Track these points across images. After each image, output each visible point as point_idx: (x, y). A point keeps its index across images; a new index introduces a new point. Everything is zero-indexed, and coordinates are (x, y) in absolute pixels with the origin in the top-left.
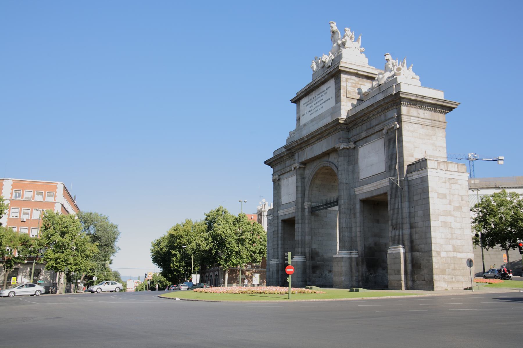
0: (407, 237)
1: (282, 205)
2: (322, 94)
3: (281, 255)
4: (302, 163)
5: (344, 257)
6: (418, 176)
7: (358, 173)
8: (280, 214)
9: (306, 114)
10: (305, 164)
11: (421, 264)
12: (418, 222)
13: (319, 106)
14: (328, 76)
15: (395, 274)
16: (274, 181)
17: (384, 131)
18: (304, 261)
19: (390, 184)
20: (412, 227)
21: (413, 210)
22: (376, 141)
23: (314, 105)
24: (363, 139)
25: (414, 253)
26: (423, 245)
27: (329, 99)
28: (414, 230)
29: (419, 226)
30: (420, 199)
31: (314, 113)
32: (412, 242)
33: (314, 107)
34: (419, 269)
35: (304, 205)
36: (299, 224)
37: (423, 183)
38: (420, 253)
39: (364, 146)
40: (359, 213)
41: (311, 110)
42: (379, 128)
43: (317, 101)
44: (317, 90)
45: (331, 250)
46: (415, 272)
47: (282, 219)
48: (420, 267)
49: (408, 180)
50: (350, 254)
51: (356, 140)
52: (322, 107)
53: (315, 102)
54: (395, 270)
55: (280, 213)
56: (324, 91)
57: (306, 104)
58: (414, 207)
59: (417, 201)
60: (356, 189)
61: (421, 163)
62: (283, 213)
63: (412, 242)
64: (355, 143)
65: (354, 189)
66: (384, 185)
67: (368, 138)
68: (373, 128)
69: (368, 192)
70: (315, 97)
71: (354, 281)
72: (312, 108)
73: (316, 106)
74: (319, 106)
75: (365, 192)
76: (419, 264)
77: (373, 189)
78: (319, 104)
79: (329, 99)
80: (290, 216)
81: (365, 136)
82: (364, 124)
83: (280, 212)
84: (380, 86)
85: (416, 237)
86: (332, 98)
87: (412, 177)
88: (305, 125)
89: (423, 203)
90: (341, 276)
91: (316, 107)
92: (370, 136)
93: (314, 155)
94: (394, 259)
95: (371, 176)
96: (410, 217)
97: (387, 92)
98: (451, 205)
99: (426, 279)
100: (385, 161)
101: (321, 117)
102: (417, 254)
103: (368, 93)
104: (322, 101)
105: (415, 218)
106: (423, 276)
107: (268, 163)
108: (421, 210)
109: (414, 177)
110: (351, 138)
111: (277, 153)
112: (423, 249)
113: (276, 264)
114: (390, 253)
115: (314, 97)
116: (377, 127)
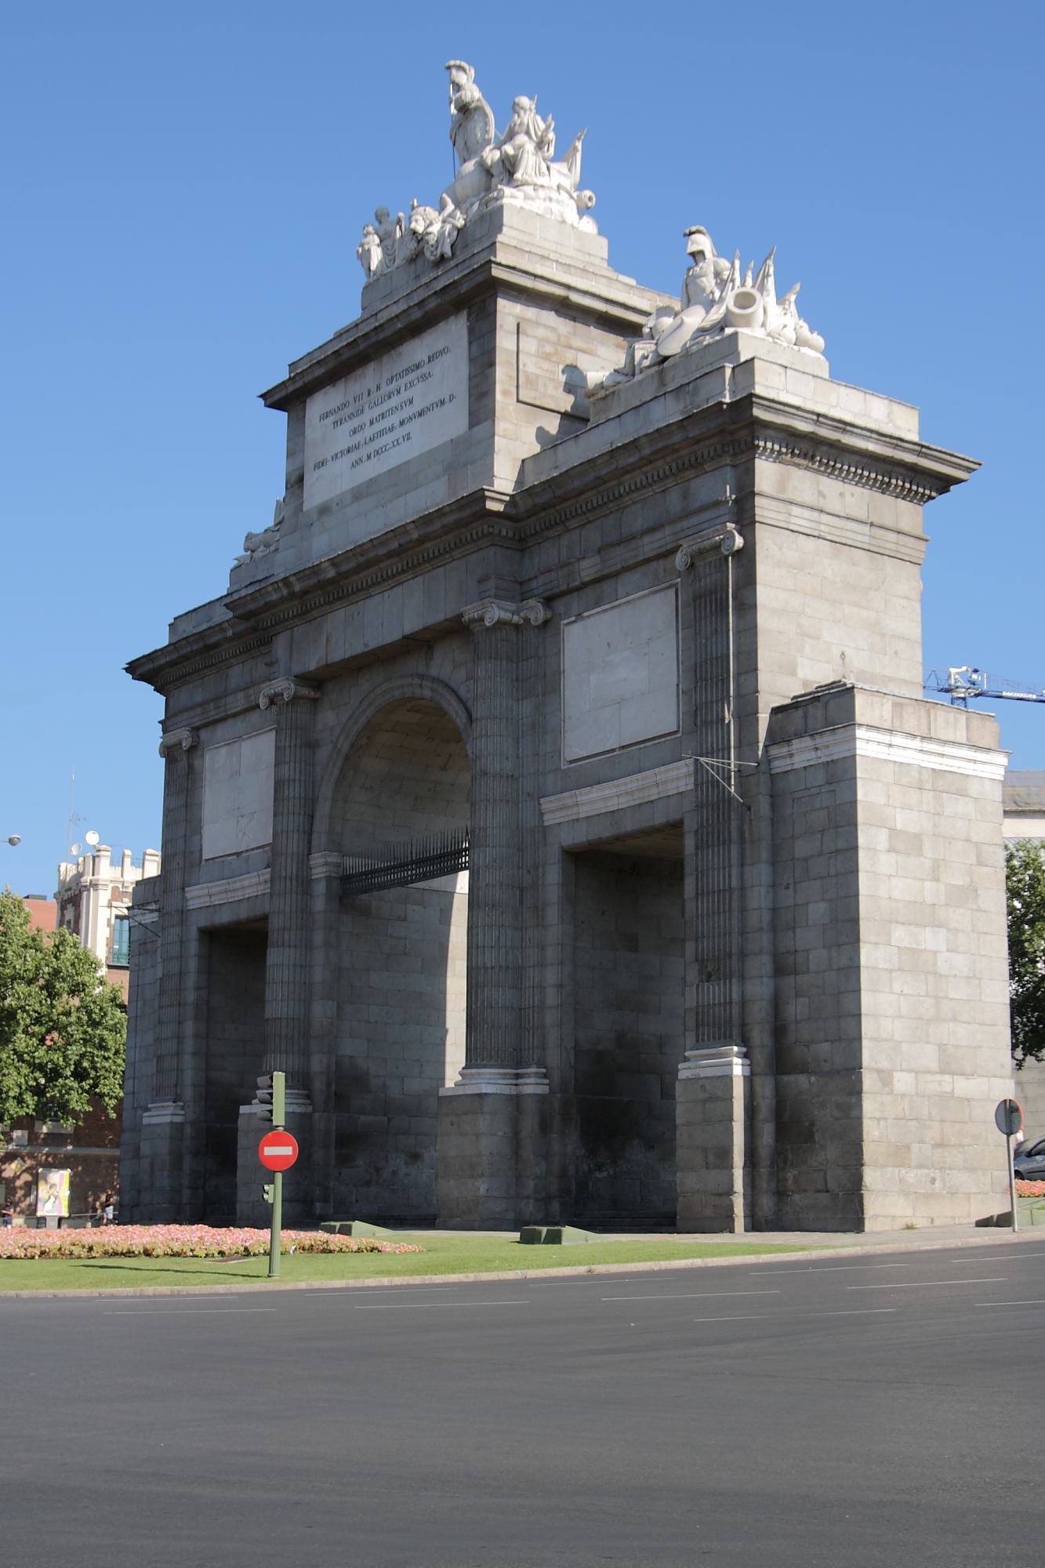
0: (759, 1011)
1: (203, 862)
3: (194, 1086)
4: (304, 679)
5: (486, 1094)
6: (813, 754)
7: (559, 732)
8: (197, 901)
9: (330, 463)
10: (318, 682)
11: (812, 1124)
12: (807, 951)
13: (392, 429)
14: (439, 300)
15: (707, 1168)
16: (169, 752)
17: (680, 560)
18: (300, 1113)
19: (696, 785)
20: (781, 969)
21: (787, 898)
22: (639, 598)
23: (372, 423)
24: (584, 585)
25: (786, 1078)
26: (826, 1046)
27: (442, 403)
28: (790, 980)
29: (812, 967)
31: (369, 457)
32: (779, 1030)
33: (369, 432)
34: (806, 1143)
35: (308, 864)
36: (292, 950)
37: (831, 788)
38: (813, 1079)
39: (588, 617)
40: (556, 906)
41: (357, 447)
42: (657, 545)
43: (384, 408)
44: (385, 358)
45: (422, 1066)
46: (790, 1157)
47: (202, 924)
48: (809, 1137)
49: (773, 772)
50: (514, 1082)
51: (557, 591)
52: (408, 437)
53: (377, 411)
54: (705, 1150)
55: (193, 898)
56: (418, 368)
57: (332, 418)
58: (791, 886)
59: (806, 859)
60: (547, 804)
61: (827, 704)
62: (208, 899)
63: (779, 1030)
64: (549, 601)
65: (539, 804)
66: (672, 789)
67: (607, 586)
69: (599, 815)
70: (378, 388)
71: (528, 1197)
72: (358, 438)
73: (378, 427)
74: (392, 429)
75: (587, 818)
76: (806, 1124)
77: (624, 802)
78: (394, 419)
79: (442, 403)
80: (244, 914)
81: (593, 577)
82: (589, 522)
83: (196, 893)
84: (666, 364)
85: (795, 1009)
86: (452, 397)
87: (788, 761)
88: (324, 510)
89: (833, 871)
90: (472, 1177)
91: (381, 433)
92: (616, 574)
93: (366, 645)
94: (705, 1101)
95: (613, 750)
96: (774, 928)
97: (696, 392)
98: (936, 879)
99: (831, 1184)
100: (678, 685)
101: (399, 479)
102: (801, 1082)
103: (611, 390)
104: (408, 411)
105: (798, 930)
106: (822, 1173)
107: (140, 669)
108: (823, 900)
109: (796, 759)
110: (530, 580)
111: (188, 629)
112: (825, 1061)
113: (172, 1122)
114: (688, 1079)
115: (373, 388)
116: (647, 539)
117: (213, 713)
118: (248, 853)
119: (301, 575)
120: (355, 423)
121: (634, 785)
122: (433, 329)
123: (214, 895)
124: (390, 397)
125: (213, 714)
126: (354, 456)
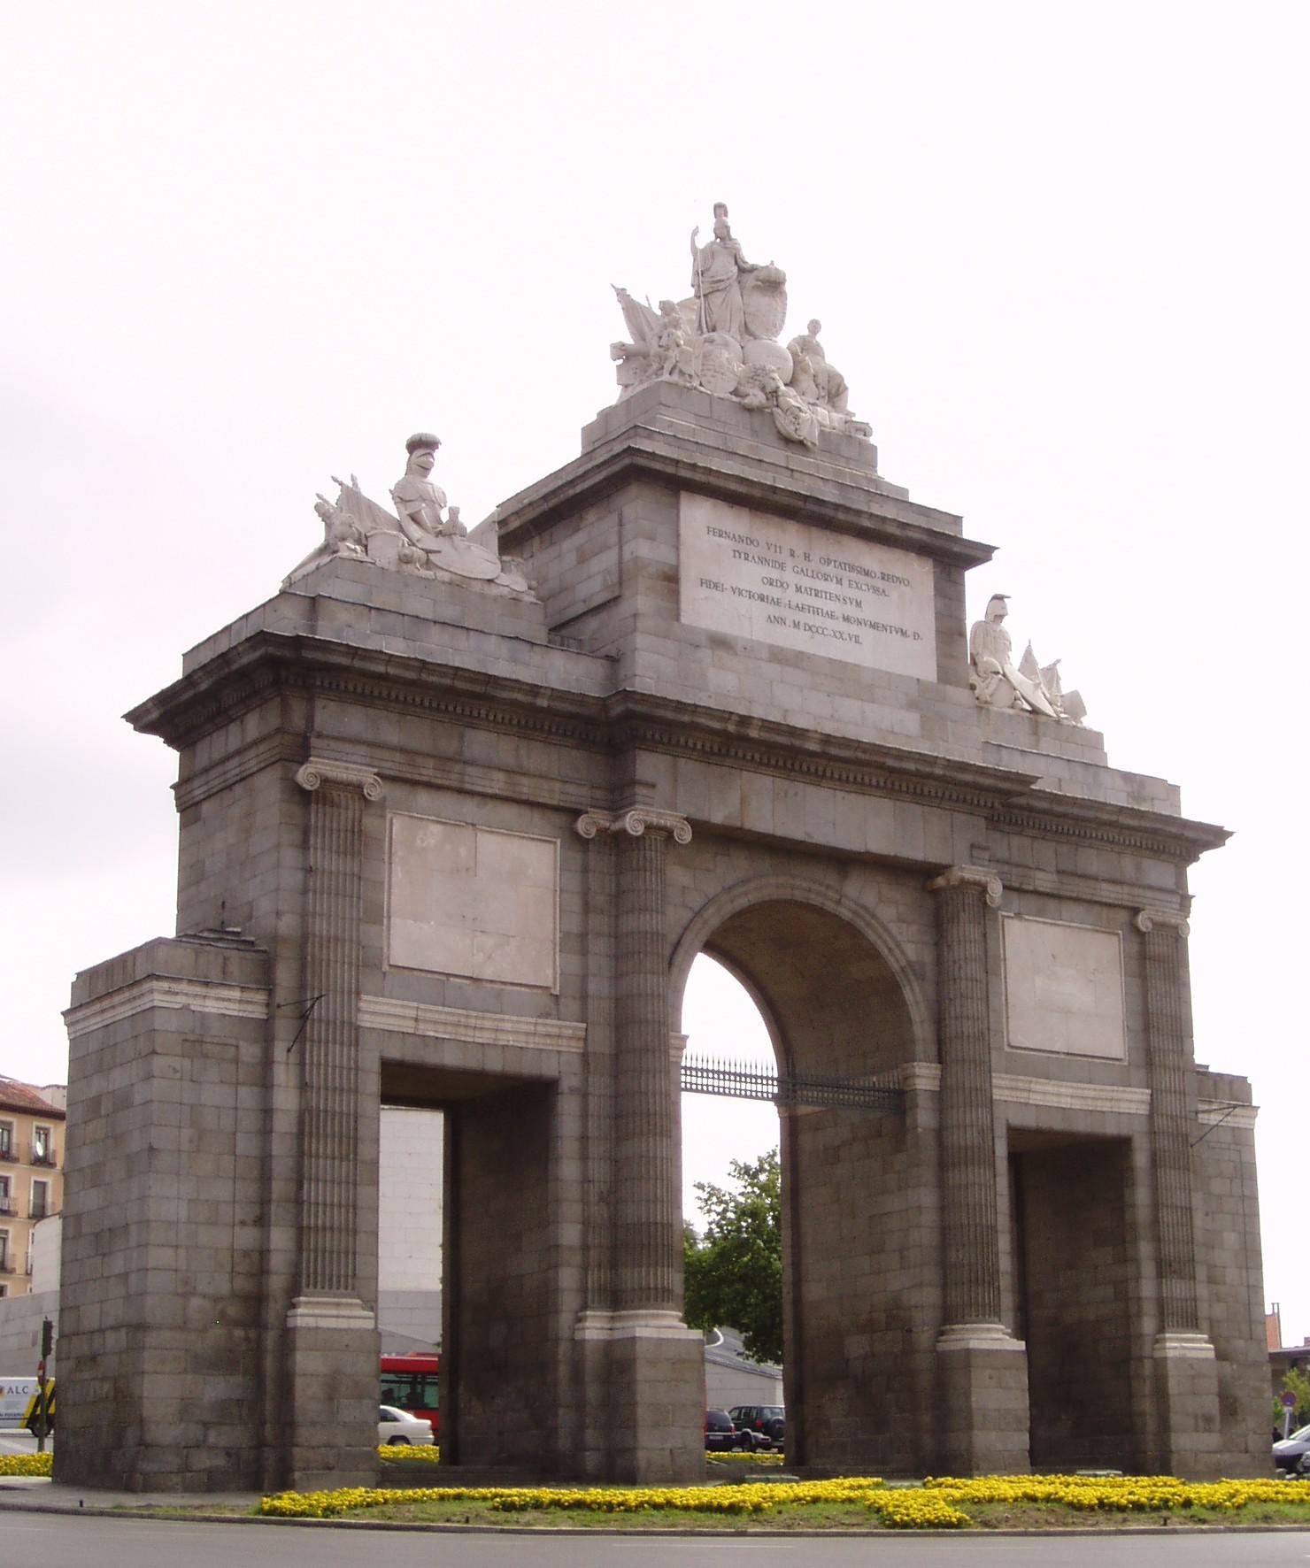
2: (854, 576)
13: (831, 616)
24: (1036, 893)
26: (1241, 1343)
27: (904, 633)
30: (1231, 1196)
33: (791, 595)
41: (777, 603)
42: (1113, 895)
47: (394, 1053)
56: (867, 573)
62: (412, 1023)
66: (1124, 1108)
67: (1052, 905)
68: (1092, 883)
70: (807, 557)
74: (831, 616)
75: (1037, 1106)
77: (1077, 1104)
79: (904, 633)
81: (1048, 890)
82: (1043, 839)
83: (372, 1008)
86: (916, 636)
88: (720, 642)
91: (816, 611)
93: (808, 834)
94: (1193, 1377)
95: (1058, 1053)
99: (1251, 1446)
101: (844, 678)
104: (851, 611)
115: (799, 552)
116: (1105, 886)
117: (431, 772)
118: (503, 987)
119: (767, 724)
120: (774, 574)
121: (1091, 1094)
122: (885, 548)
123: (425, 1021)
124: (826, 580)
125: (428, 771)
126: (774, 611)
